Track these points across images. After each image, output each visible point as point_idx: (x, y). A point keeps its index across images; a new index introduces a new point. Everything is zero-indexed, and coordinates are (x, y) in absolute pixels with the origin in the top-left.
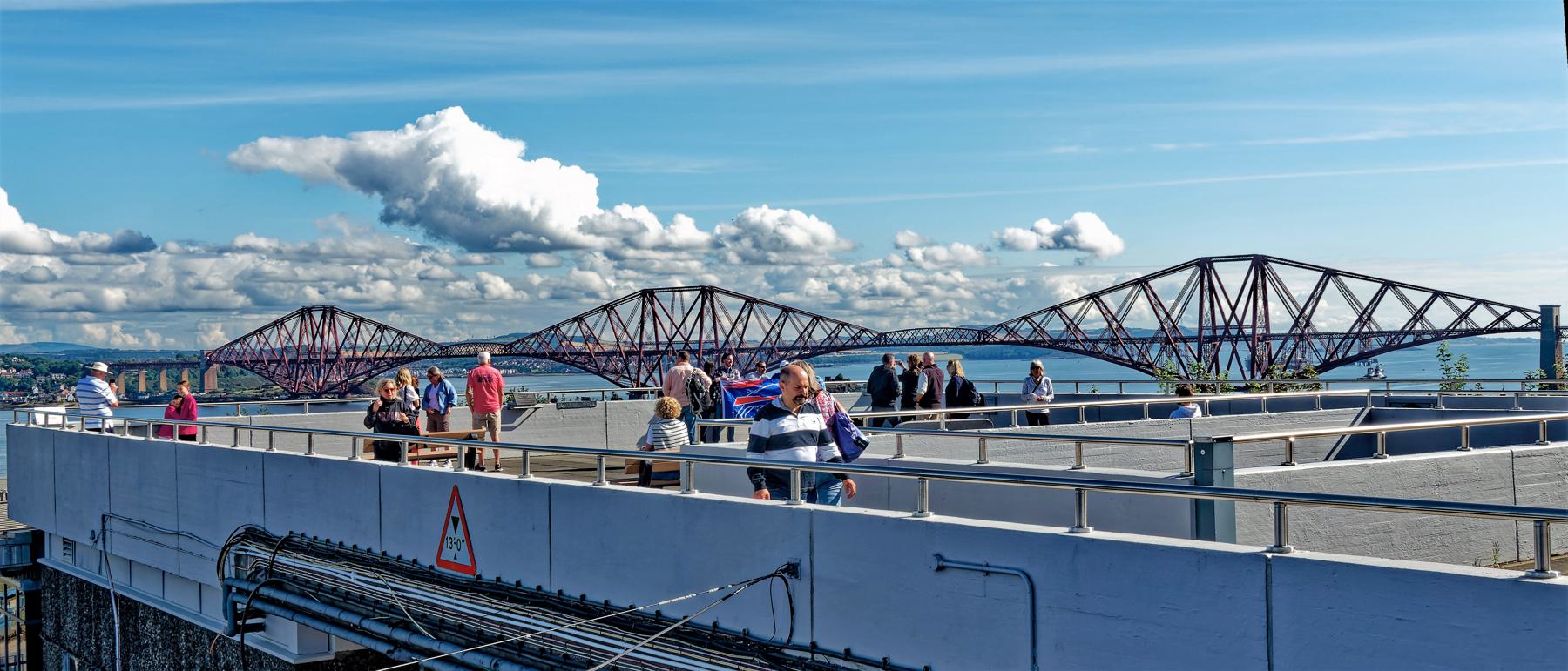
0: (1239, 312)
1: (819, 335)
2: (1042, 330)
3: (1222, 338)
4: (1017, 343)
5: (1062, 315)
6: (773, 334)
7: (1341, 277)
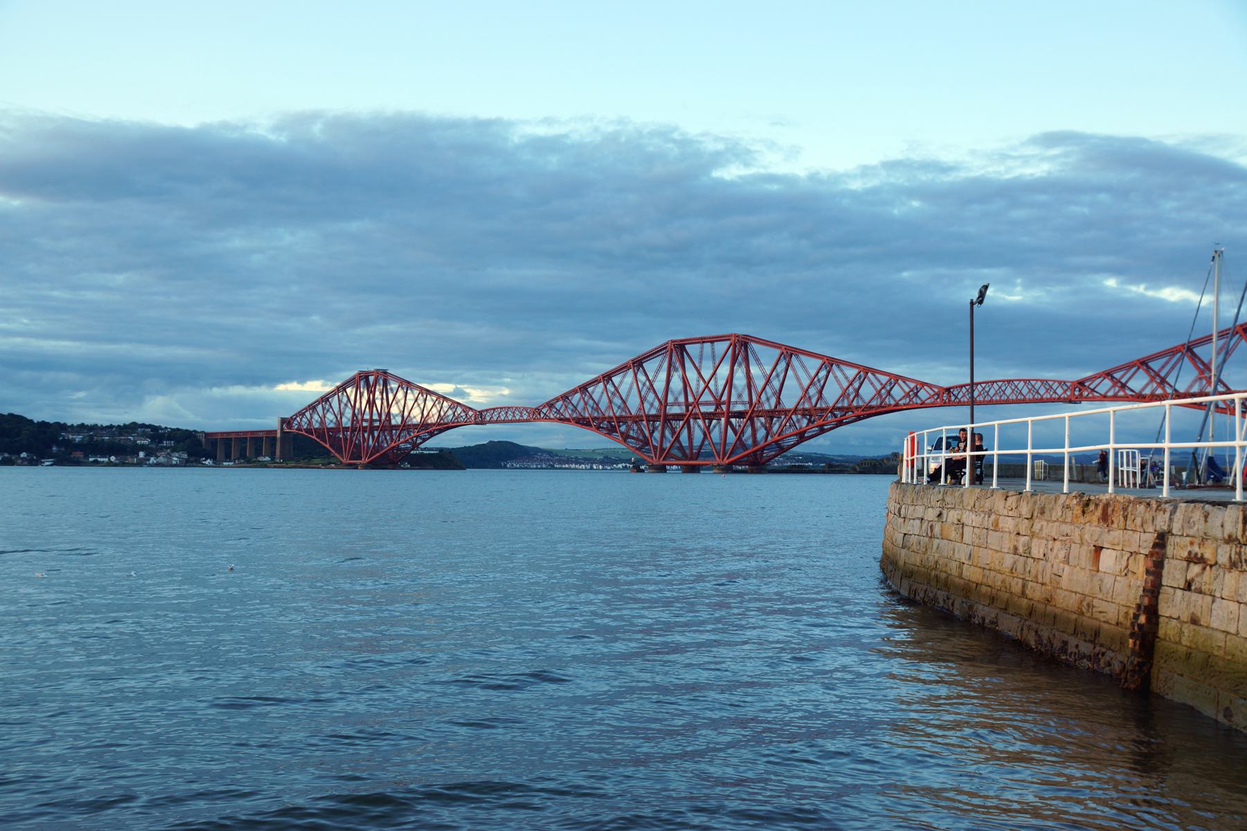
5: (1194, 357)
6: (812, 391)
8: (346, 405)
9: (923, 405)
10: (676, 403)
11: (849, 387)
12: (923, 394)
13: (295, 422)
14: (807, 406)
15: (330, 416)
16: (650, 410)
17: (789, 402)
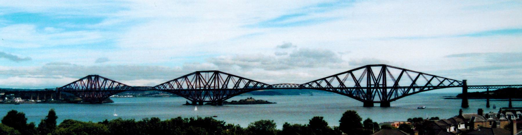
0: (378, 82)
1: (251, 85)
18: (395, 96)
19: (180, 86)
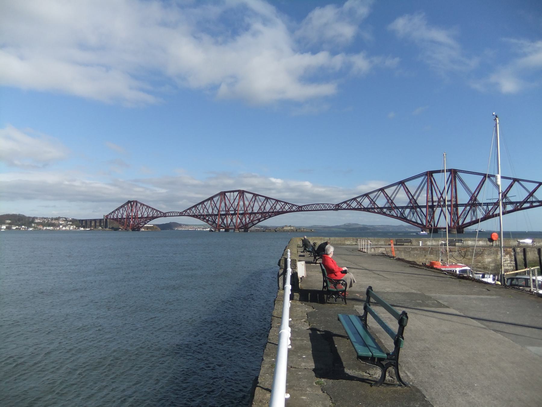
2: (361, 204)
3: (439, 206)
4: (351, 209)
6: (262, 207)
7: (491, 177)
8: (124, 211)
9: (294, 211)
10: (223, 211)
11: (273, 206)
12: (294, 208)
13: (109, 216)
14: (261, 211)
15: (120, 214)
16: (215, 212)
17: (255, 210)
18: (472, 219)
19: (413, 201)
